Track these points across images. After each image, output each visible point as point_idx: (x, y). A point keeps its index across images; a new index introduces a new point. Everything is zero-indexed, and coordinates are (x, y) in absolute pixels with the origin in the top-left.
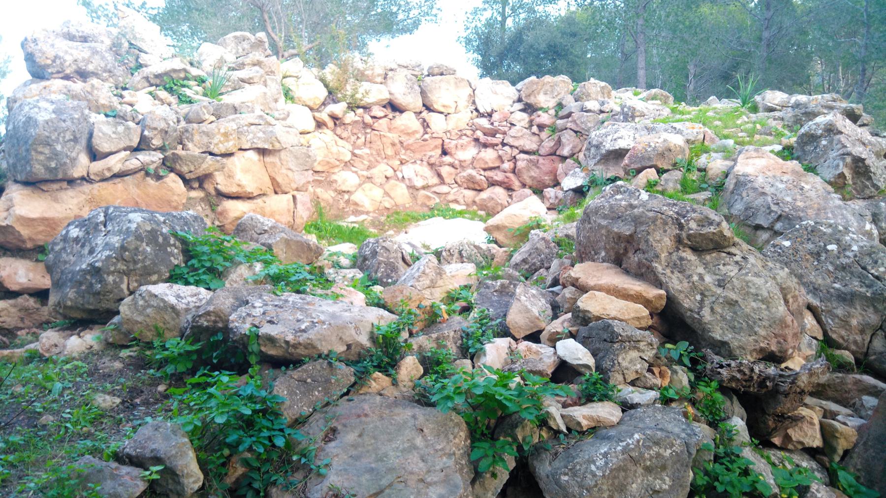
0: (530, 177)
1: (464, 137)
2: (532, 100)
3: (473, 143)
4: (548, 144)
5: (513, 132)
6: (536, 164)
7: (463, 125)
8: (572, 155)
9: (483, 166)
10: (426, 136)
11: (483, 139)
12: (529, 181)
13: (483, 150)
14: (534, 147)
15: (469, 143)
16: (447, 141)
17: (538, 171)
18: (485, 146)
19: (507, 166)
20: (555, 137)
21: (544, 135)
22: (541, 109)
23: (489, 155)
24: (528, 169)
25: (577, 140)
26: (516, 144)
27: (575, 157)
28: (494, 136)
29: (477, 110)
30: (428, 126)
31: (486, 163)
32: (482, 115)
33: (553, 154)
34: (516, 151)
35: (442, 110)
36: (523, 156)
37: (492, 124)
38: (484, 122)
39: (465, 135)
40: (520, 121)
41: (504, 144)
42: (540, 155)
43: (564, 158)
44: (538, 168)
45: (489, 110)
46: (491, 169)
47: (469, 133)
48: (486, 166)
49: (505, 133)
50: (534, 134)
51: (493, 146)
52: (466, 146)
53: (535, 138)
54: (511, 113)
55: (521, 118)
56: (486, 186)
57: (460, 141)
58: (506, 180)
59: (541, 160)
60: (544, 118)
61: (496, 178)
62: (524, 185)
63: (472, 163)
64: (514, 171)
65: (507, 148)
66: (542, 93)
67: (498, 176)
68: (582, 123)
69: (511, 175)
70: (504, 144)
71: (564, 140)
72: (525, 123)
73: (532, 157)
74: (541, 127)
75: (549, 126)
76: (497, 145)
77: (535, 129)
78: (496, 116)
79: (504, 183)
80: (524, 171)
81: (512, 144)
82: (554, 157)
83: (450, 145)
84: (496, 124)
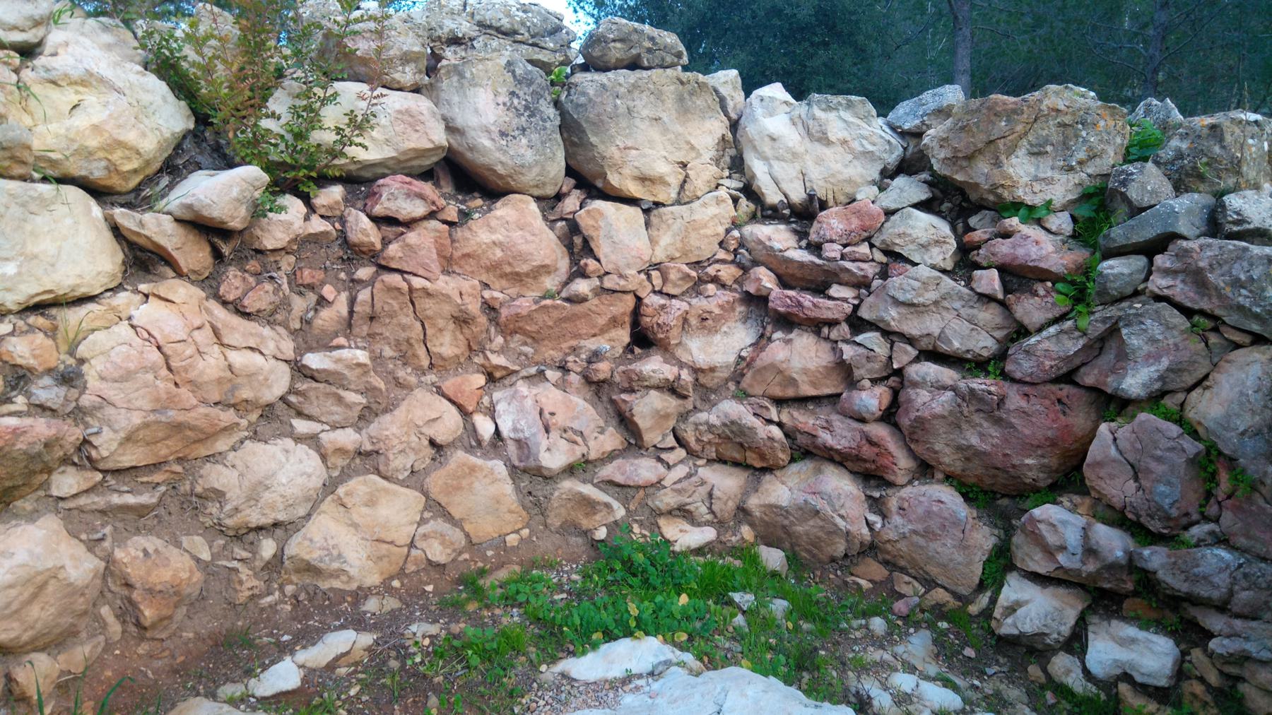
0: (959, 448)
1: (711, 288)
2: (980, 173)
3: (740, 309)
4: (1052, 347)
5: (901, 284)
6: (992, 409)
7: (705, 246)
8: (1154, 399)
9: (778, 392)
10: (582, 287)
11: (780, 298)
12: (949, 459)
13: (778, 335)
14: (984, 344)
15: (727, 308)
16: (654, 301)
17: (994, 432)
18: (787, 322)
19: (872, 399)
20: (1095, 321)
21: (1031, 309)
22: (1016, 207)
23: (801, 356)
24: (955, 421)
25: (1197, 345)
26: (913, 327)
27: (1170, 402)
28: (820, 289)
29: (750, 191)
30: (588, 250)
31: (793, 382)
32: (768, 213)
33: (1068, 378)
34: (904, 354)
35: (634, 189)
36: (931, 370)
37: (816, 248)
38: (778, 236)
39: (715, 280)
40: (924, 247)
41: (857, 324)
42: (1005, 376)
43: (1114, 405)
44: (998, 421)
45: (798, 196)
46: (802, 401)
47: (728, 273)
48: (790, 393)
49: (862, 284)
50: (986, 298)
51: (817, 326)
52: (718, 319)
53: (989, 315)
54: (889, 213)
55: (926, 233)
56: (783, 457)
57: (699, 303)
58: (867, 451)
59: (1015, 399)
60: (1042, 246)
61: (826, 438)
62: (925, 470)
63: (737, 377)
64: (889, 416)
65: (870, 338)
66: (1021, 152)
67: (840, 435)
68: (1237, 284)
69: (880, 431)
70: (857, 324)
71: (1133, 339)
72: (945, 254)
73: (979, 384)
74: (1019, 277)
75: (1056, 278)
76: (832, 323)
77: (989, 281)
78: (832, 223)
79: (858, 459)
80: (941, 427)
81: (894, 325)
82: (1066, 390)
83: (667, 313)
84: (832, 251)
